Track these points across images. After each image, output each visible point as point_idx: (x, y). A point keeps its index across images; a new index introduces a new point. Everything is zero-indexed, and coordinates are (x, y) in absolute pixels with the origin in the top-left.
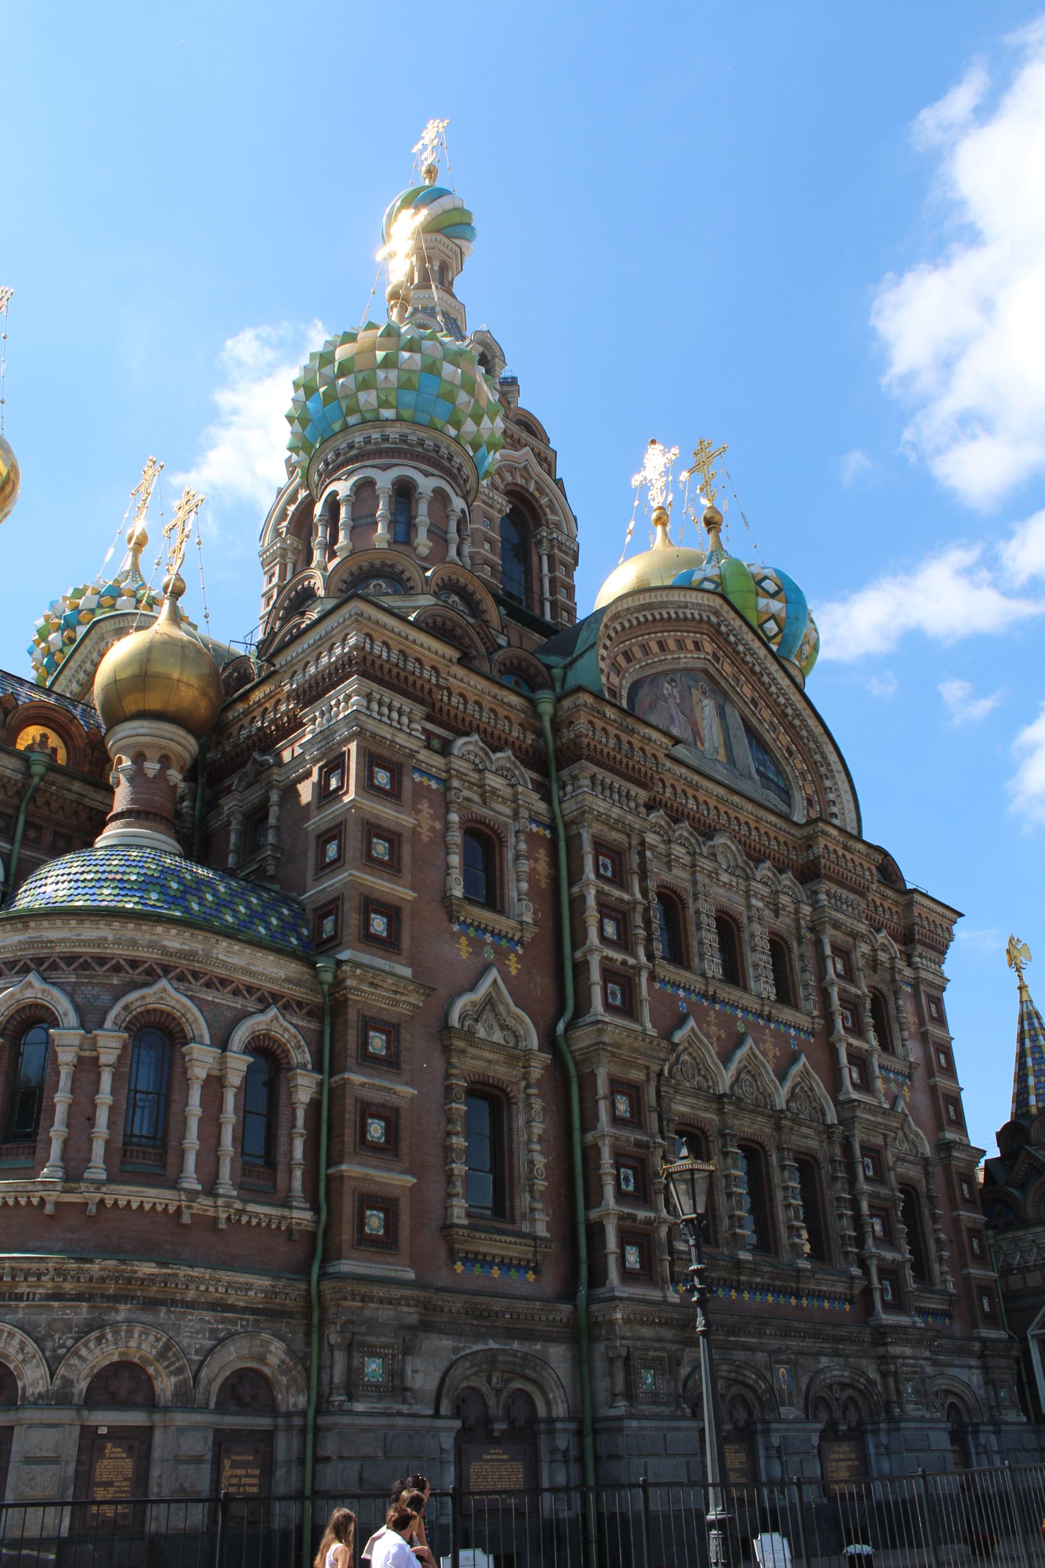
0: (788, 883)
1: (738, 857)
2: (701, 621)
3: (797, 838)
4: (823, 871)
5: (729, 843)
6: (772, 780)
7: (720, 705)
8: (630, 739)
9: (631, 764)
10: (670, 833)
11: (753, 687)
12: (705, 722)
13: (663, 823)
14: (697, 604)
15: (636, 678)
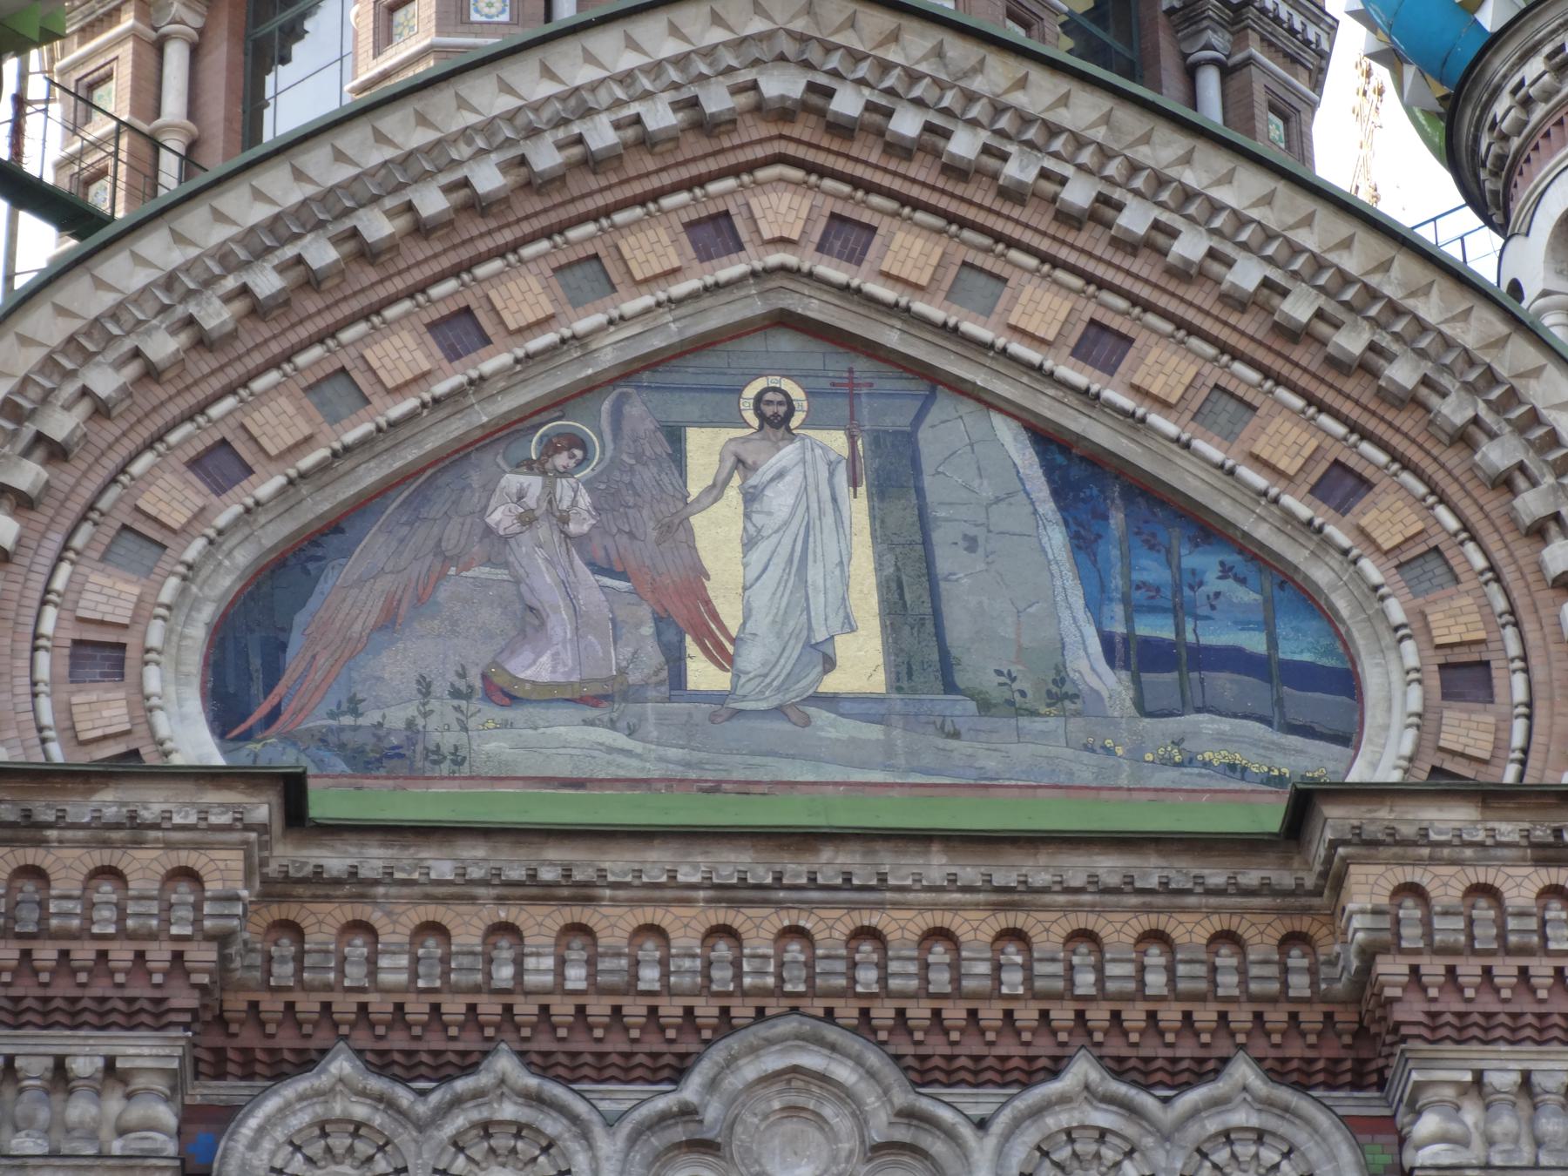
0: (1241, 1117)
1: (871, 1100)
2: (705, 126)
3: (1298, 891)
4: (1410, 1010)
5: (813, 1060)
6: (1234, 660)
7: (877, 440)
8: (31, 856)
9: (46, 953)
10: (405, 1137)
11: (1089, 279)
12: (758, 555)
13: (360, 1111)
14: (656, 68)
15: (274, 532)
